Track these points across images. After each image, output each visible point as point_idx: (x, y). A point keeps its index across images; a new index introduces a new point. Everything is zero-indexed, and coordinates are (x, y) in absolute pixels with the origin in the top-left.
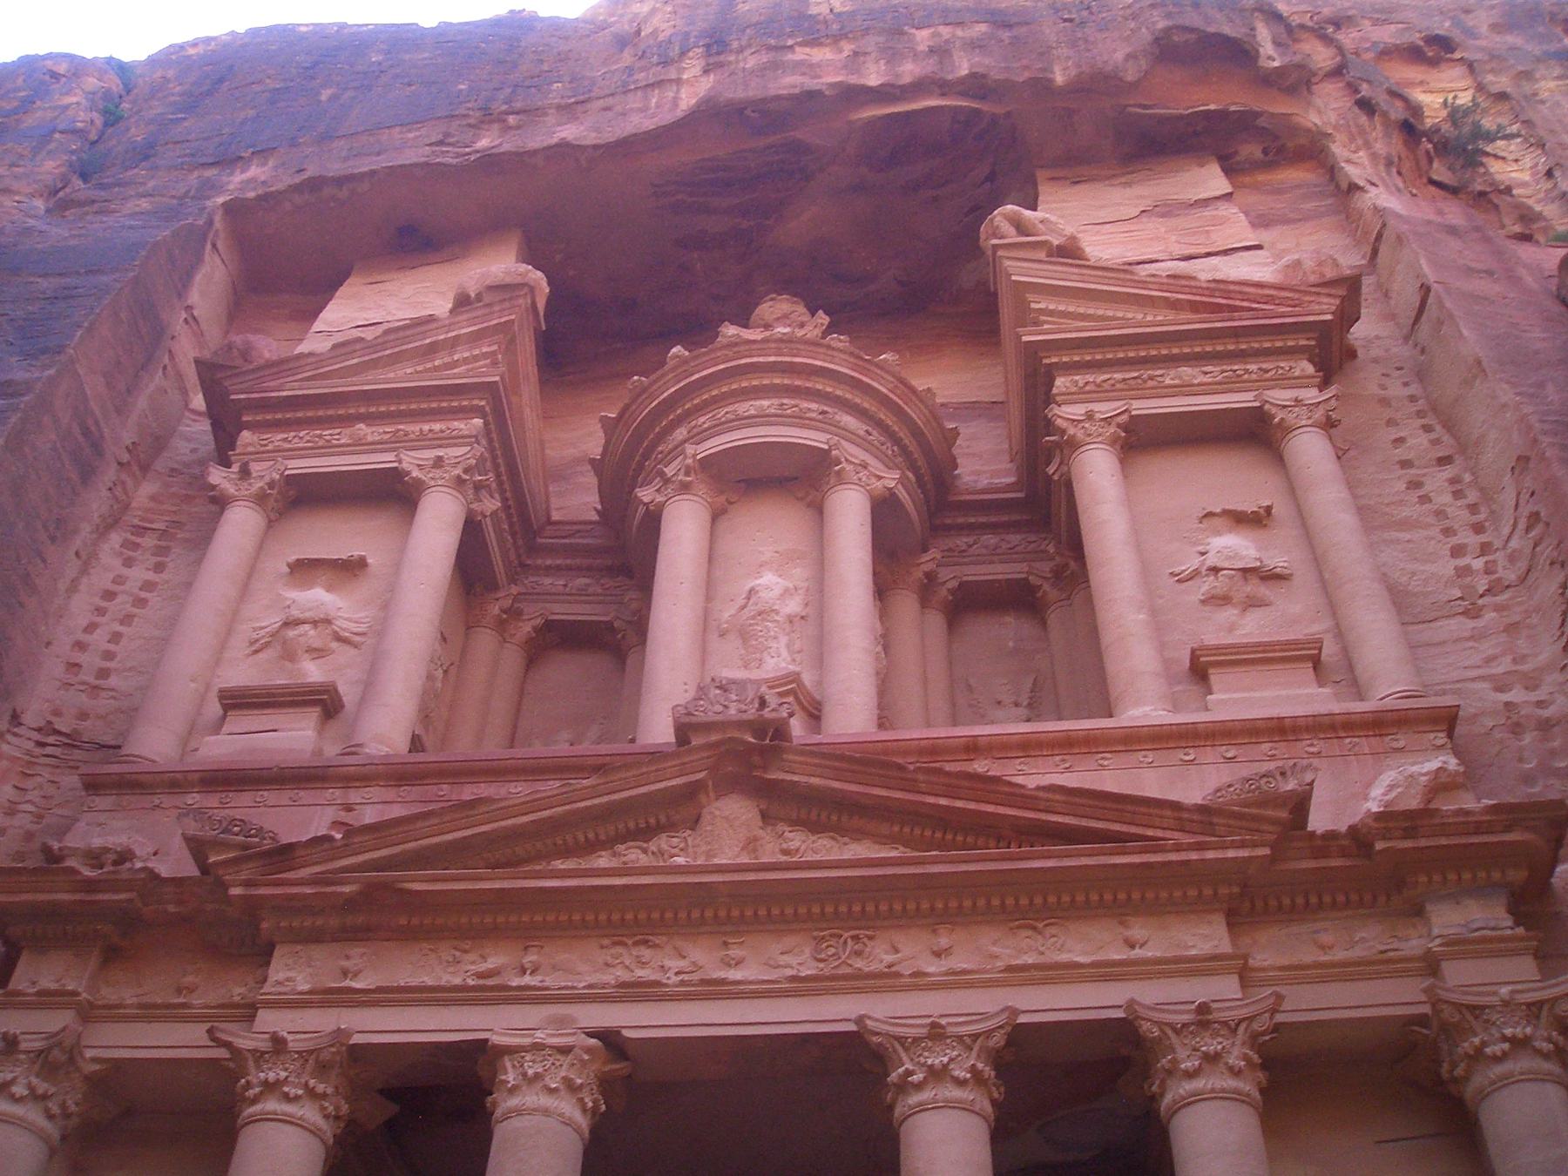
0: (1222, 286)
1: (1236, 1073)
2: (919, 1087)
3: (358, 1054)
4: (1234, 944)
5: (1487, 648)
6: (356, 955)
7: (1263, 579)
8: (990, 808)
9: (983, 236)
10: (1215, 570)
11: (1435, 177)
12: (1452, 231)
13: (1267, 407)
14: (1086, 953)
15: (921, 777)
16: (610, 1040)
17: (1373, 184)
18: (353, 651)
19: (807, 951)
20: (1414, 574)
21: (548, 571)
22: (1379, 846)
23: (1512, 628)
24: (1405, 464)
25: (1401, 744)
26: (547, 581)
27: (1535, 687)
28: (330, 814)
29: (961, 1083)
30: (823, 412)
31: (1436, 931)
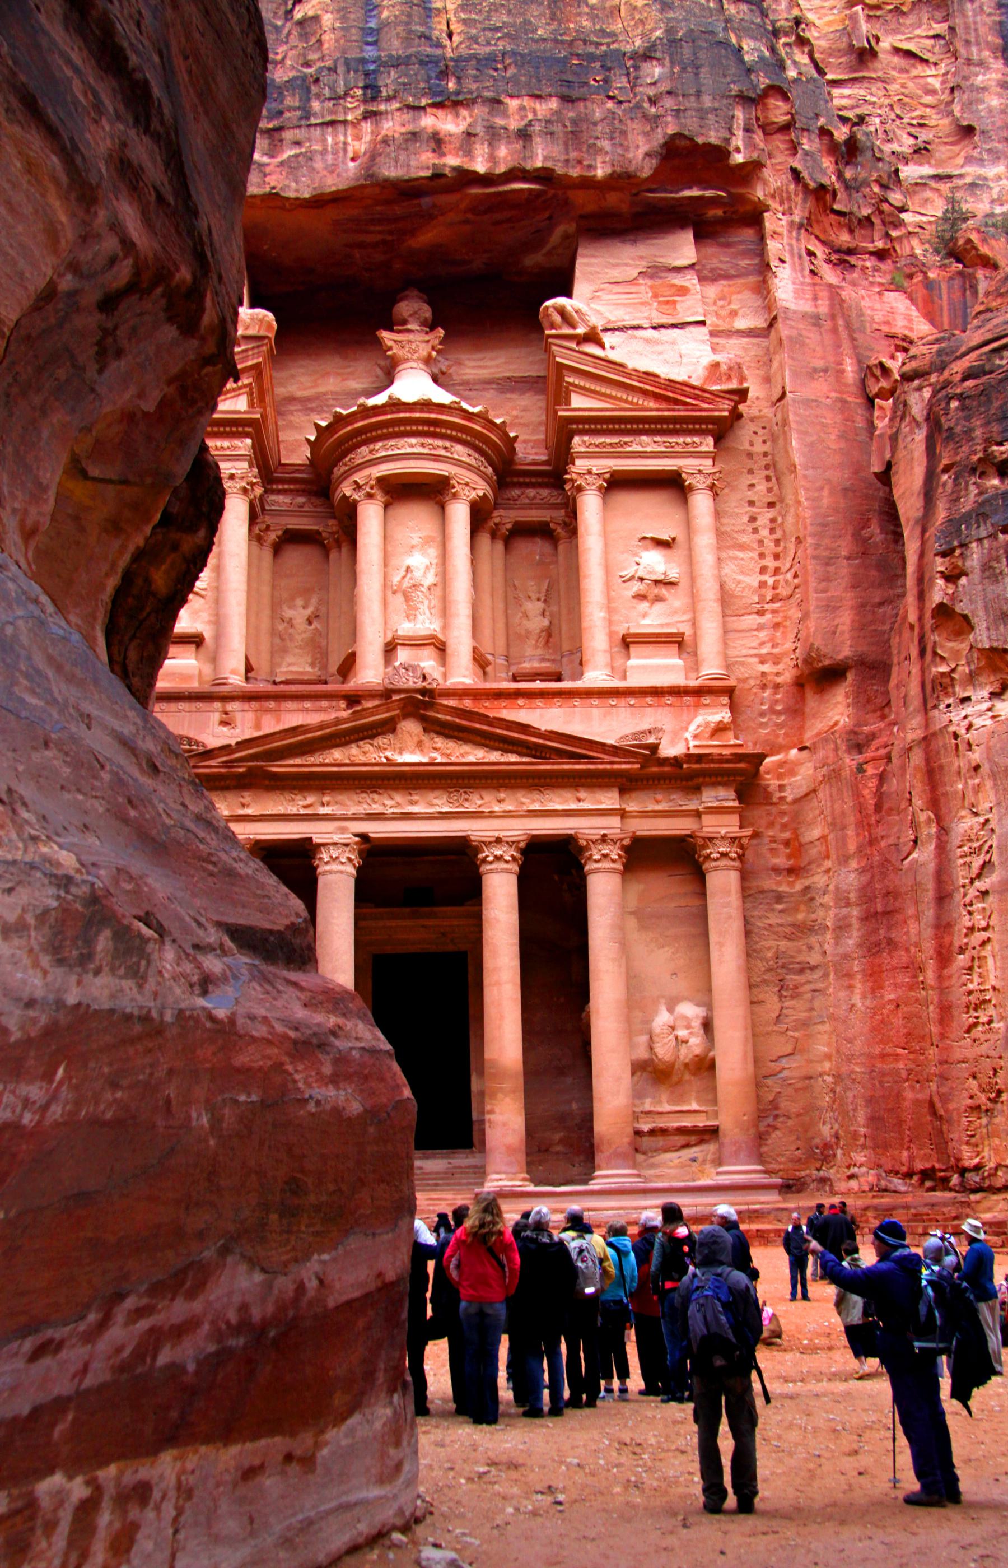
1: (613, 861)
2: (491, 863)
3: (258, 842)
5: (763, 635)
6: (247, 797)
7: (666, 584)
8: (523, 737)
10: (641, 579)
11: (835, 207)
12: (815, 320)
13: (684, 475)
16: (364, 837)
17: (782, 261)
18: (202, 601)
20: (739, 582)
21: (279, 492)
23: (776, 626)
24: (751, 503)
25: (707, 702)
26: (281, 498)
28: (216, 717)
29: (507, 862)
30: (446, 448)
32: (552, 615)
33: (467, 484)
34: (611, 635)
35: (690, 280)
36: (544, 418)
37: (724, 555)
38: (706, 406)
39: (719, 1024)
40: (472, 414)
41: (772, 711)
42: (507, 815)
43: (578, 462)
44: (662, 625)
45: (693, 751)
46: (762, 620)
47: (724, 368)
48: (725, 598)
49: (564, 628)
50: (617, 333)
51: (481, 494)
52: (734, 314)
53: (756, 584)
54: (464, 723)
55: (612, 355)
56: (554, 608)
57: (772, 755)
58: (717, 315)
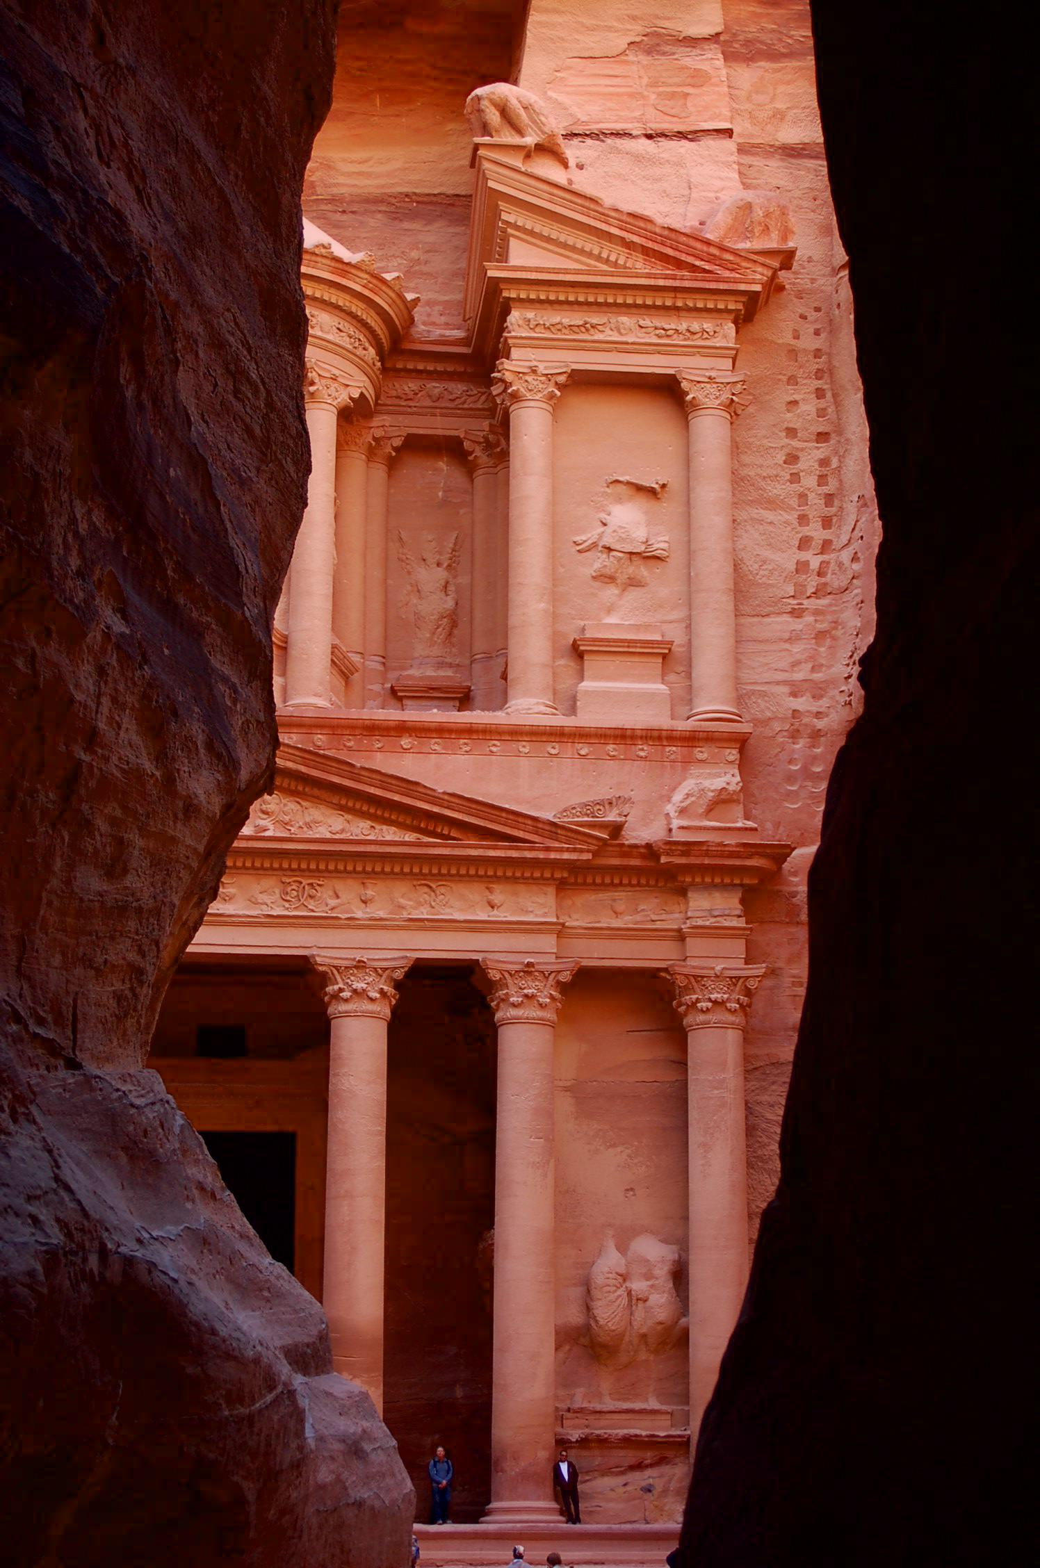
0: (673, 235)
2: (346, 1000)
4: (559, 906)
5: (797, 648)
9: (467, 110)
10: (609, 549)
13: (684, 385)
14: (461, 910)
15: (363, 773)
19: (277, 891)
22: (663, 860)
23: (820, 636)
24: (791, 432)
25: (706, 755)
27: (821, 697)
31: (690, 914)
32: (457, 592)
33: (334, 379)
34: (555, 636)
35: (711, 61)
36: (463, 265)
37: (742, 515)
38: (727, 274)
39: (699, 1273)
40: (348, 264)
41: (807, 774)
42: (376, 924)
43: (515, 353)
44: (637, 627)
45: (678, 836)
46: (797, 625)
47: (759, 213)
48: (742, 587)
49: (479, 615)
50: (589, 141)
51: (356, 396)
52: (779, 116)
53: (793, 567)
54: (315, 773)
55: (583, 182)
56: (464, 580)
57: (803, 845)
58: (751, 116)
